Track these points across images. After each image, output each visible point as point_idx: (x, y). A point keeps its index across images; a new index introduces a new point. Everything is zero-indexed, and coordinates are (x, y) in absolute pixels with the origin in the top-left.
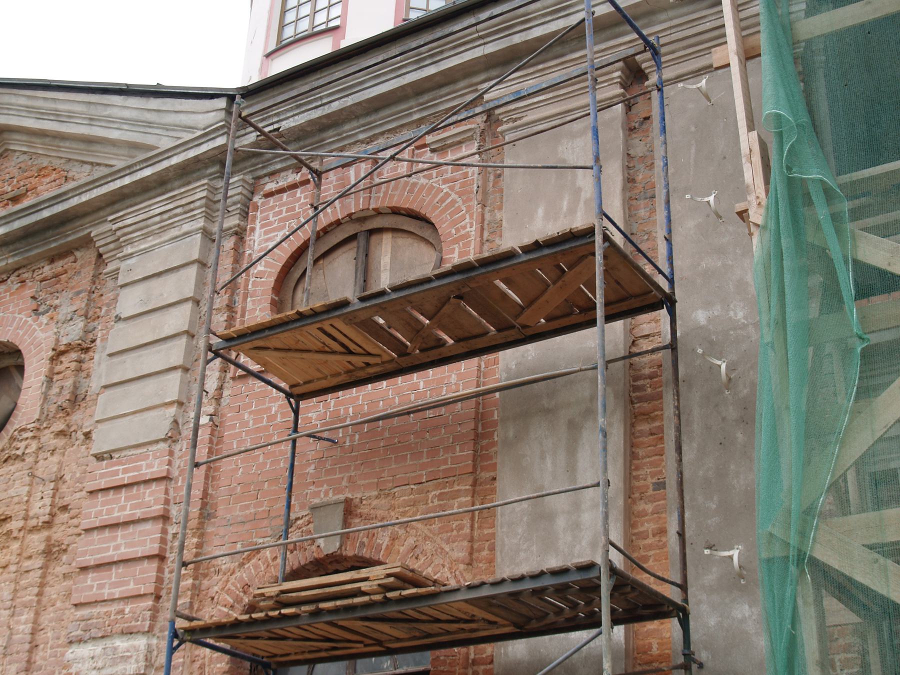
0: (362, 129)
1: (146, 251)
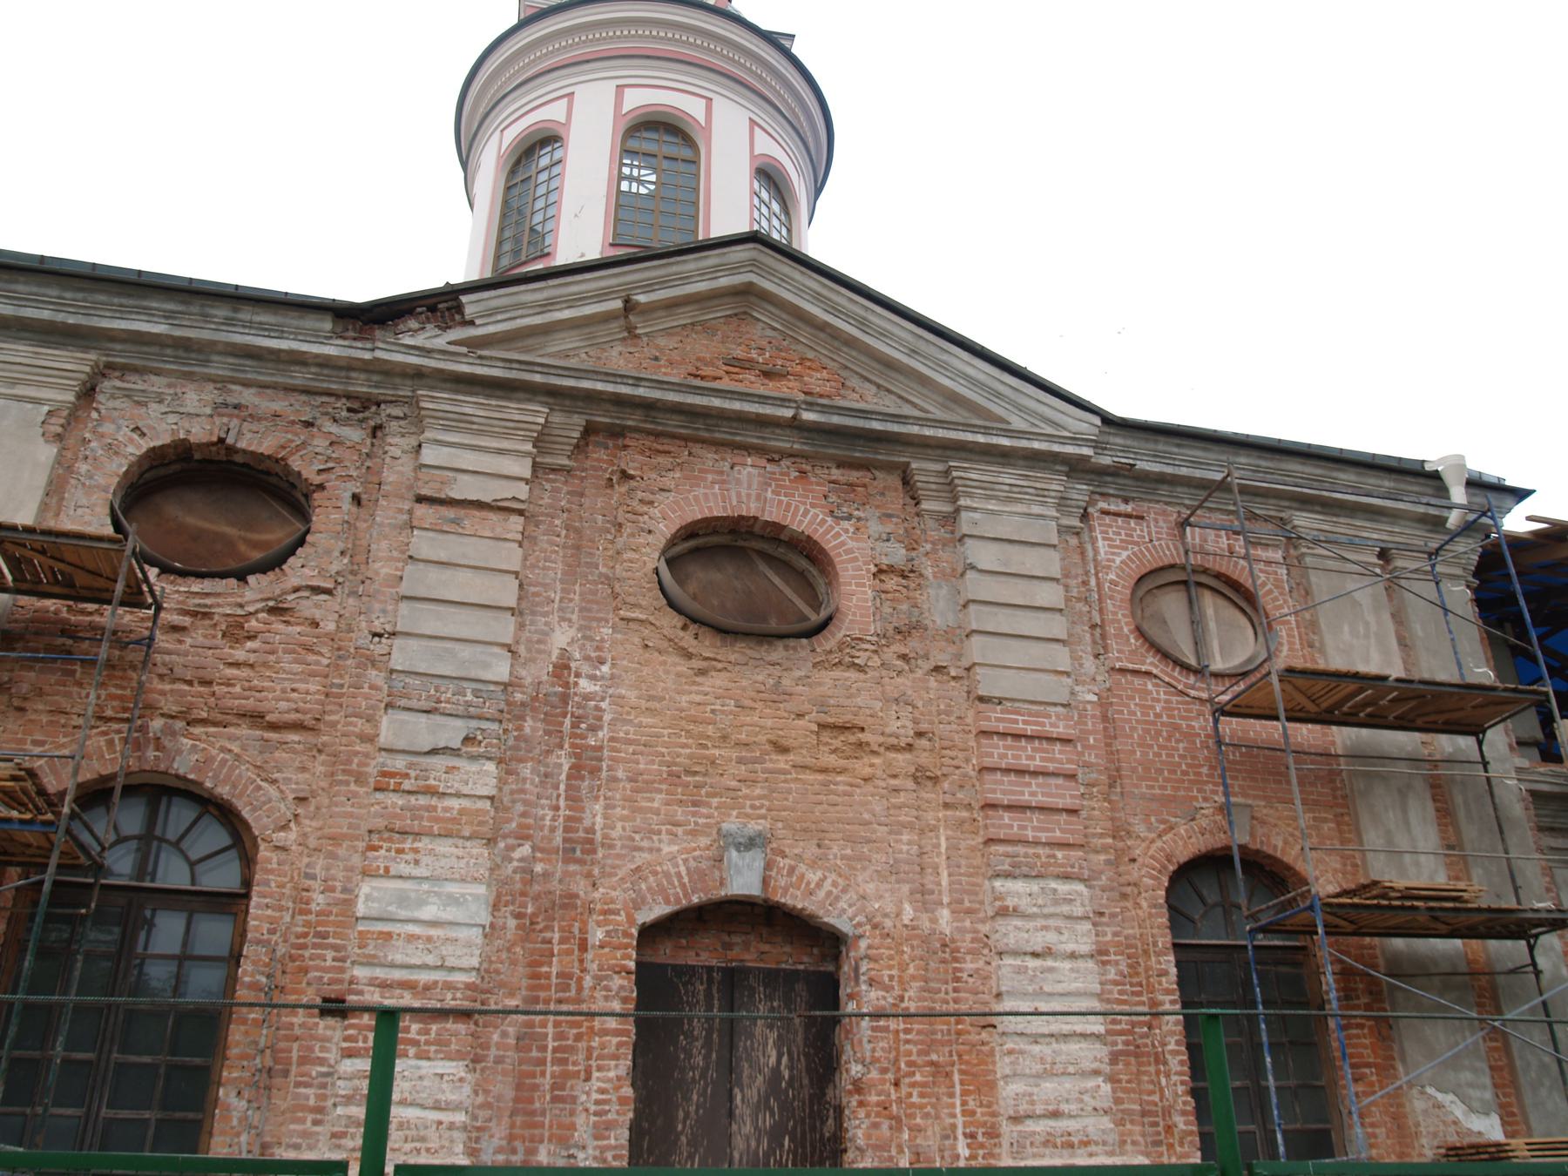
1: (993, 512)
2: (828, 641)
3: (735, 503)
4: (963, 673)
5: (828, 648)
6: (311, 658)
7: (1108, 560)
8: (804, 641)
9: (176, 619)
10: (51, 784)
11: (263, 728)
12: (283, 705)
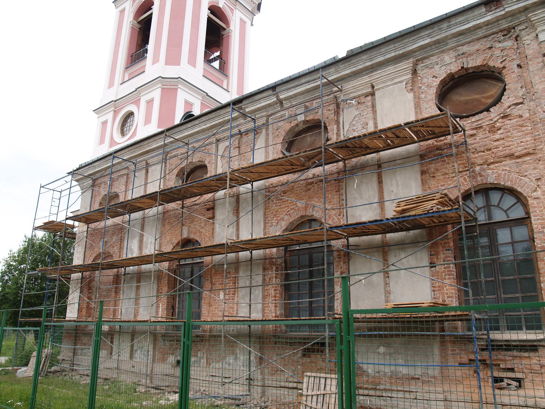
6: (524, 129)
9: (471, 132)
10: (452, 197)
11: (515, 159)
12: (519, 148)
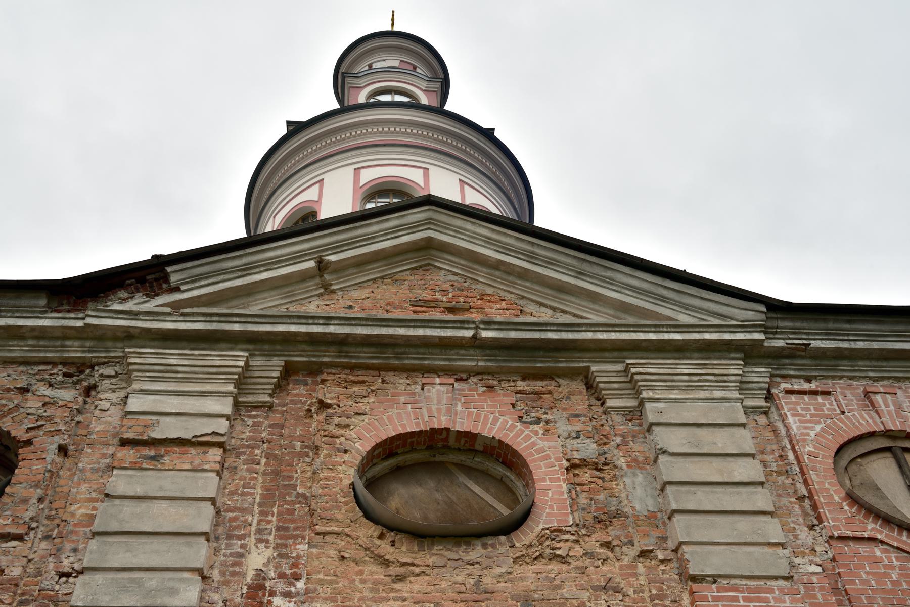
0: (873, 369)
1: (676, 401)
2: (526, 536)
3: (426, 418)
4: (672, 556)
5: (527, 543)
7: (802, 434)
8: (503, 538)
